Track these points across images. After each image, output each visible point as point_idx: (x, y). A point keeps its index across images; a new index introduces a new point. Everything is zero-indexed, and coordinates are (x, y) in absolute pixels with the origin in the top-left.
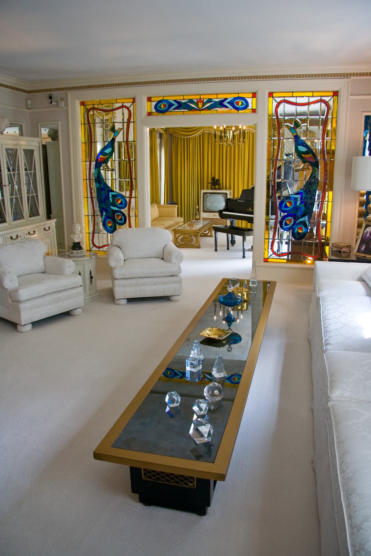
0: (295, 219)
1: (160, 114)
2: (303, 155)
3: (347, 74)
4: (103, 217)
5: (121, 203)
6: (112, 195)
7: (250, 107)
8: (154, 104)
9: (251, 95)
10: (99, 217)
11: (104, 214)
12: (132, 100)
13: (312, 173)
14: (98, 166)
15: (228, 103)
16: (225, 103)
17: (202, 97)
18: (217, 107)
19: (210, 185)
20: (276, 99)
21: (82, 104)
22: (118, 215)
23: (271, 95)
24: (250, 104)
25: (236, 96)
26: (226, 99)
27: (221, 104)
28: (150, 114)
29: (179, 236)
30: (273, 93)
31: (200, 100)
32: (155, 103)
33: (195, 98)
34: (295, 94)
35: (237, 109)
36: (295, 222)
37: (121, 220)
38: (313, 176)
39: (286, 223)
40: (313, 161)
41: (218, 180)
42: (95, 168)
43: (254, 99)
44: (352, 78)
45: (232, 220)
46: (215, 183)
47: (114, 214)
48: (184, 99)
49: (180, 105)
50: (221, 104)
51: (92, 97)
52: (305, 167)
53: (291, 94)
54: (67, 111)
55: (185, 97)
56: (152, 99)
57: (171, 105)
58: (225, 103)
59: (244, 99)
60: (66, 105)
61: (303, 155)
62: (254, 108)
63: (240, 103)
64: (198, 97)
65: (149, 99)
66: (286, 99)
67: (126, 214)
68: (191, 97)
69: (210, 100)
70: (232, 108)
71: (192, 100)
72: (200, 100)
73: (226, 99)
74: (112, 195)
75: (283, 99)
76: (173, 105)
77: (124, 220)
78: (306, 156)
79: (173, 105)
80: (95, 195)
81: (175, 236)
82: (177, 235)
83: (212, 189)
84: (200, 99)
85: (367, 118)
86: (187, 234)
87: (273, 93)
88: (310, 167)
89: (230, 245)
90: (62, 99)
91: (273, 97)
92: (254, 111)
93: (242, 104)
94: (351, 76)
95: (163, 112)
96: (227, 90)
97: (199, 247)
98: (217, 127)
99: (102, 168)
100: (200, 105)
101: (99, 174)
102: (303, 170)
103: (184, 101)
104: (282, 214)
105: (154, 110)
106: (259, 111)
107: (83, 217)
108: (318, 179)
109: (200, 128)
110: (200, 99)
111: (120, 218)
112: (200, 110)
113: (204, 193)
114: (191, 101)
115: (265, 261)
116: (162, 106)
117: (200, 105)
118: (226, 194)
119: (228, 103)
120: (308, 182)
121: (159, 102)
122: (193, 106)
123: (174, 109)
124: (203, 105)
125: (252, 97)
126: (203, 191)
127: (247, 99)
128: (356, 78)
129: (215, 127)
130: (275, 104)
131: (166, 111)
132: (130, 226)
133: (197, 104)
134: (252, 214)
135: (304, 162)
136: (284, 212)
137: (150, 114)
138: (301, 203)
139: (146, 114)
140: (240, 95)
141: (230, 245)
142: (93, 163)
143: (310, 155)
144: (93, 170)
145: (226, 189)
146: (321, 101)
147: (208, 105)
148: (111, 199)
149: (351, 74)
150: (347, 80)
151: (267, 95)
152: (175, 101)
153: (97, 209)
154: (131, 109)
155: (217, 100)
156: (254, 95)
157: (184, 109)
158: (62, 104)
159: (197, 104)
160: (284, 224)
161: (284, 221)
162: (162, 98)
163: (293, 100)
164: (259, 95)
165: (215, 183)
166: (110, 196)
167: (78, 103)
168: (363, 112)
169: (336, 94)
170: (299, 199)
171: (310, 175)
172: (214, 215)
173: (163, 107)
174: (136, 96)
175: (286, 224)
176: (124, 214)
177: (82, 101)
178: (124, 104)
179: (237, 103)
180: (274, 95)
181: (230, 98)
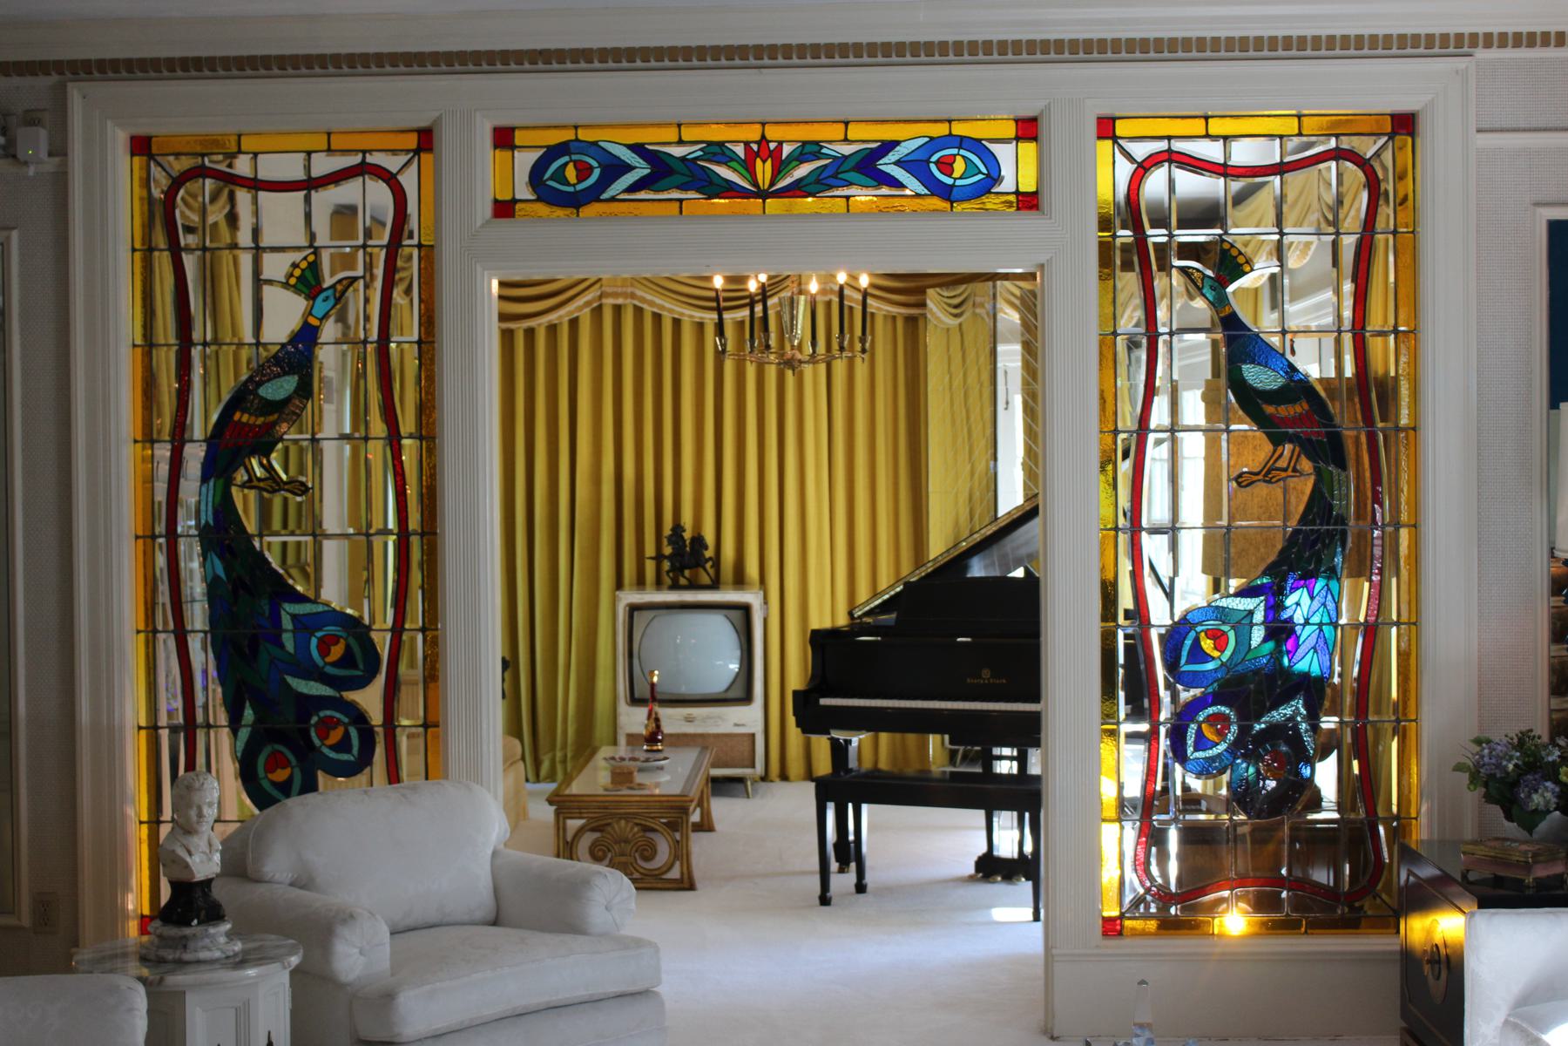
0: (1248, 715)
1: (560, 212)
2: (1269, 409)
3: (1459, 37)
4: (244, 733)
5: (347, 660)
6: (295, 618)
7: (1007, 185)
8: (525, 161)
9: (1010, 130)
10: (225, 733)
11: (249, 714)
12: (412, 141)
13: (1316, 490)
14: (218, 467)
15: (898, 163)
16: (887, 165)
17: (773, 133)
18: (850, 184)
19: (650, 567)
20: (1132, 147)
21: (141, 146)
22: (327, 726)
23: (1106, 128)
24: (1007, 171)
25: (940, 130)
26: (888, 146)
27: (868, 166)
28: (504, 209)
29: (580, 832)
30: (1113, 120)
31: (763, 149)
32: (534, 156)
33: (738, 137)
34: (1216, 127)
35: (946, 193)
36: (1244, 731)
37: (343, 745)
38: (1319, 506)
39: (1199, 733)
40: (1316, 431)
41: (698, 541)
42: (205, 479)
43: (1028, 149)
44: (1481, 54)
45: (840, 735)
46: (686, 560)
47: (304, 717)
48: (681, 142)
49: (661, 171)
50: (868, 166)
51: (184, 111)
52: (1282, 463)
53: (1197, 127)
54: (60, 183)
55: (687, 134)
56: (519, 138)
57: (614, 168)
58: (887, 165)
59: (976, 145)
60: (59, 150)
61: (1269, 409)
62: (1028, 185)
63: (959, 167)
64: (753, 134)
65: (504, 138)
66: (1178, 146)
67: (376, 718)
68: (716, 134)
69: (809, 150)
70: (922, 190)
71: (721, 144)
72: (763, 149)
73: (888, 146)
74: (295, 618)
75: (1163, 145)
76: (629, 168)
77: (362, 750)
78: (1284, 411)
79: (629, 168)
80: (198, 616)
81: (560, 827)
82: (574, 824)
83: (675, 586)
84: (763, 140)
85: (1559, 232)
86: (627, 817)
87: (1113, 120)
88: (1306, 465)
89: (834, 866)
90: (31, 120)
91: (1115, 139)
92: (1028, 201)
93: (970, 169)
94: (1474, 44)
95: (575, 201)
96: (889, 108)
97: (686, 884)
98: (729, 279)
99: (241, 476)
100: (764, 170)
101: (225, 511)
102: (1268, 474)
103: (678, 151)
104: (1186, 695)
105: (524, 192)
106: (1054, 199)
107: (130, 732)
108: (1342, 520)
109: (576, 287)
110: (763, 140)
111: (336, 736)
112: (763, 195)
113: (633, 609)
114: (718, 151)
115: (1105, 934)
116: (571, 173)
117: (764, 170)
118: (746, 609)
119: (898, 163)
120: (1296, 532)
121: (553, 152)
122: (724, 172)
123: (633, 188)
124: (780, 168)
125: (1018, 139)
126: (630, 597)
127: (993, 147)
128: (1495, 53)
129: (718, 282)
130: (1125, 170)
131: (593, 195)
132: (394, 776)
133: (748, 166)
134: (1035, 697)
135: (1277, 440)
136: (1191, 680)
137: (504, 209)
138: (1265, 640)
139: (488, 210)
140: (959, 129)
141: (834, 866)
142: (195, 455)
143: (1300, 408)
144: (191, 488)
145: (740, 581)
146: (1337, 155)
147: (802, 171)
148: (288, 641)
149: (1474, 37)
150: (1461, 63)
151: (1092, 128)
152: (638, 149)
153: (211, 695)
154: (408, 181)
155: (847, 150)
156: (1028, 129)
157: (683, 187)
158: (34, 144)
159: (748, 166)
160: (1190, 741)
161: (1193, 728)
162: (568, 135)
163: (1211, 151)
164: (1053, 129)
165: (686, 560)
166: (287, 623)
167: (119, 140)
168: (1537, 204)
169: (1404, 124)
170: (1259, 617)
171: (1301, 508)
172: (689, 720)
173: (573, 179)
174: (438, 121)
175: (1201, 743)
176: (359, 718)
177: (142, 131)
178: (370, 159)
179: (946, 166)
180: (1121, 128)
181: (911, 140)
